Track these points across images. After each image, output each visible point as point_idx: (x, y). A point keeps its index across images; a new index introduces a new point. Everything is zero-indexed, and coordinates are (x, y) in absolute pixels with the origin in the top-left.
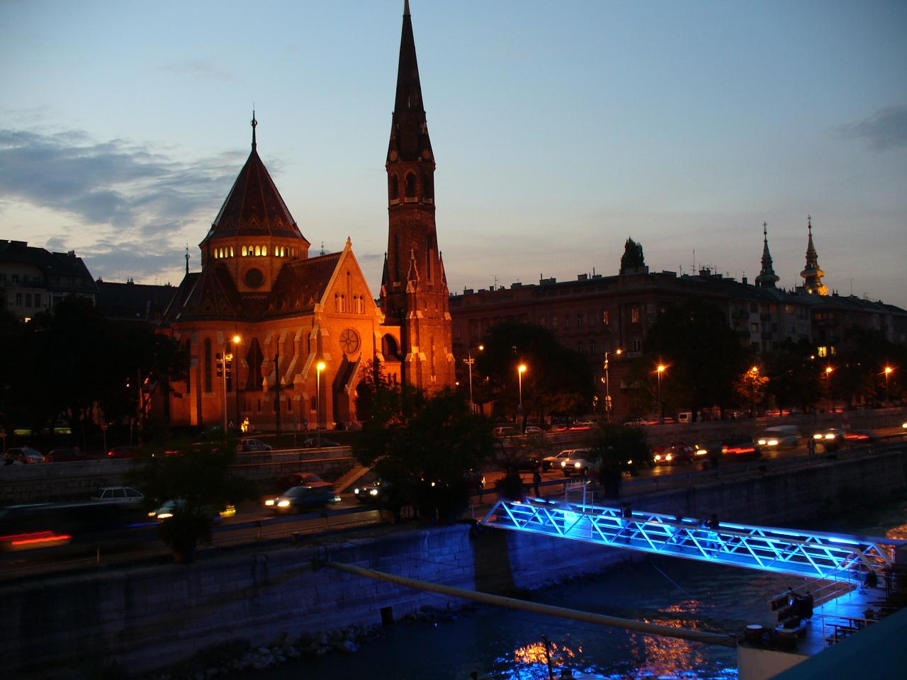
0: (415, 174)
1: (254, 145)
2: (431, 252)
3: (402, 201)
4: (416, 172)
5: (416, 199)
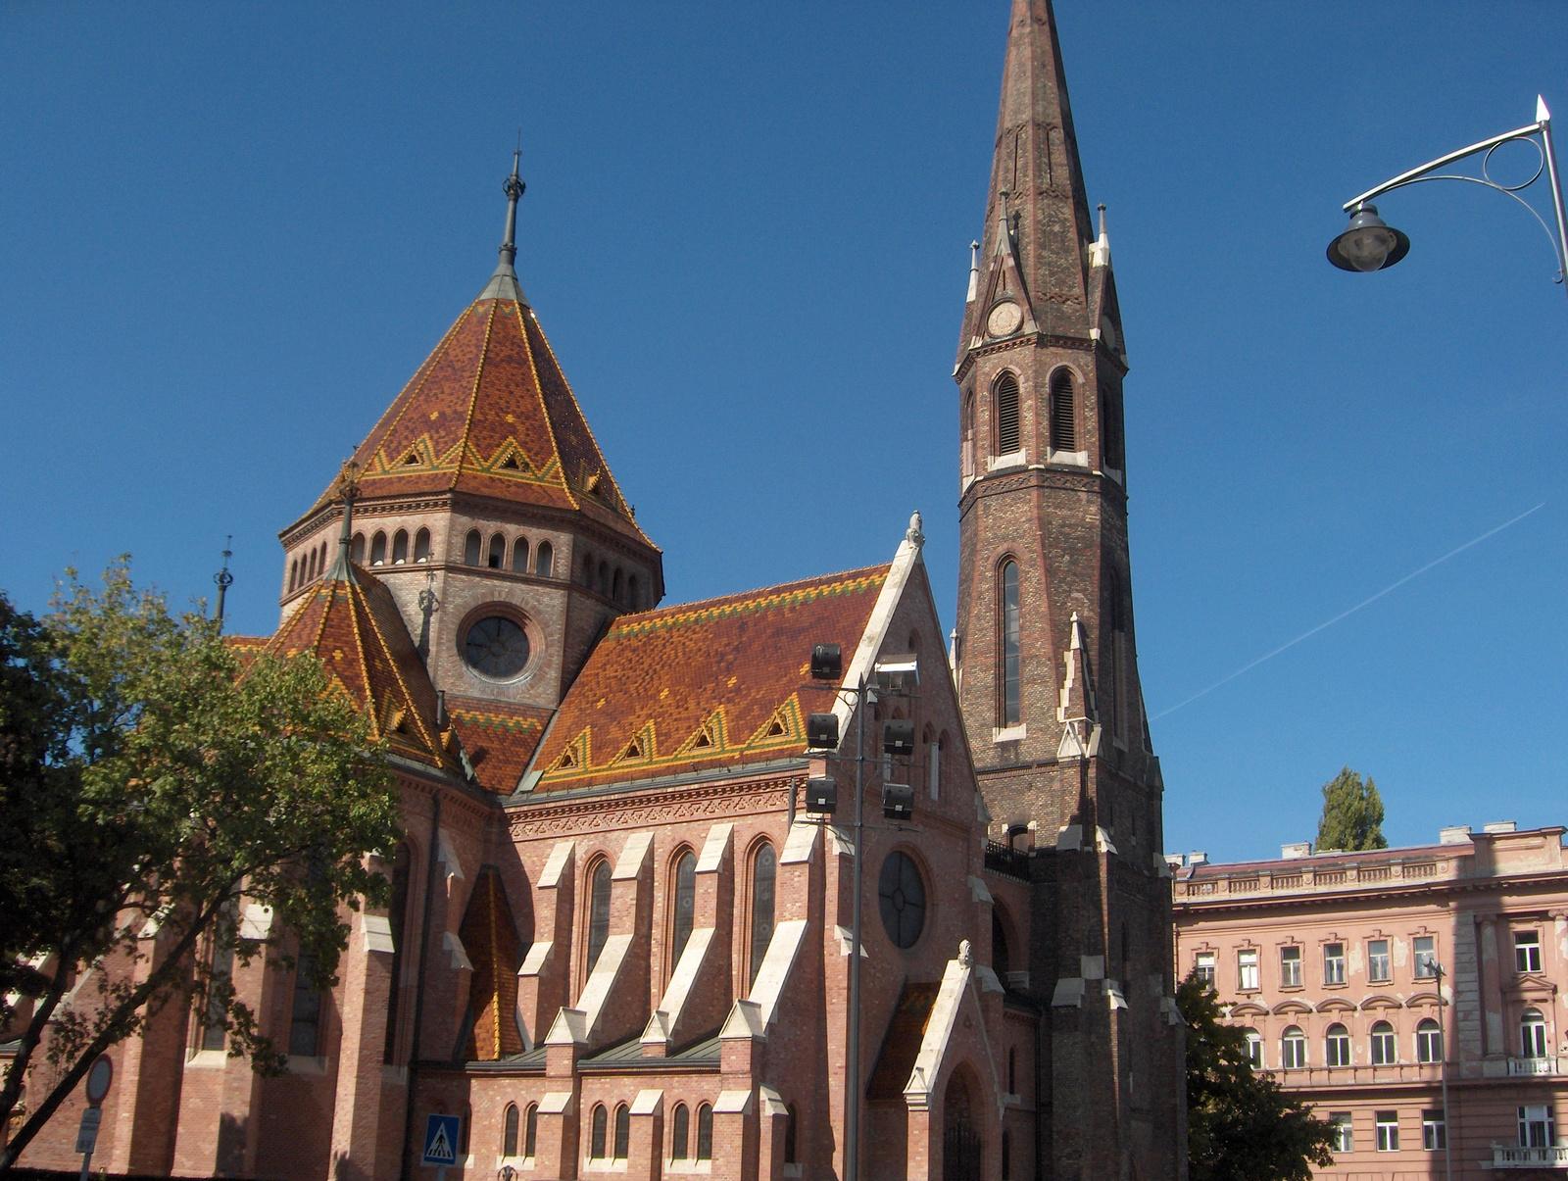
0: (1080, 380)
3: (1040, 456)
4: (1085, 375)
5: (1081, 458)
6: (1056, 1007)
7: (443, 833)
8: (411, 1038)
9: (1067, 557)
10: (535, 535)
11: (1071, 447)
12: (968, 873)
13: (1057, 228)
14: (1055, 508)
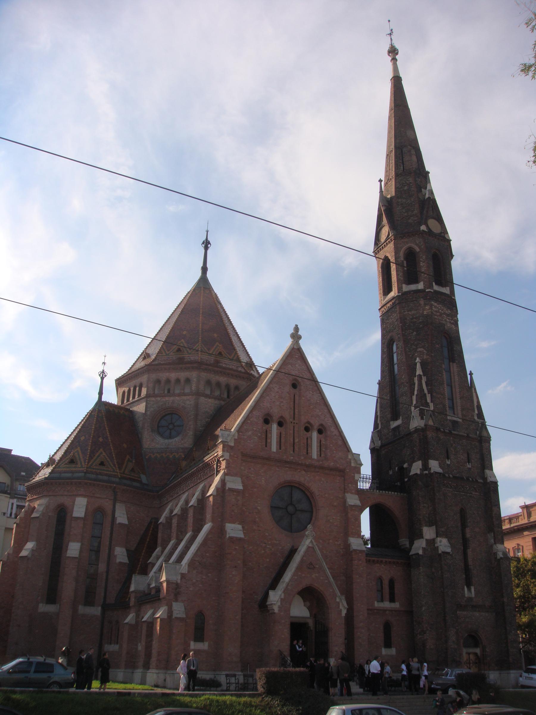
0: (418, 250)
1: (204, 269)
2: (454, 368)
4: (419, 247)
5: (420, 286)
6: (412, 555)
7: (118, 505)
8: (103, 594)
9: (415, 333)
10: (183, 375)
11: (416, 282)
12: (344, 492)
13: (406, 188)
14: (408, 311)
